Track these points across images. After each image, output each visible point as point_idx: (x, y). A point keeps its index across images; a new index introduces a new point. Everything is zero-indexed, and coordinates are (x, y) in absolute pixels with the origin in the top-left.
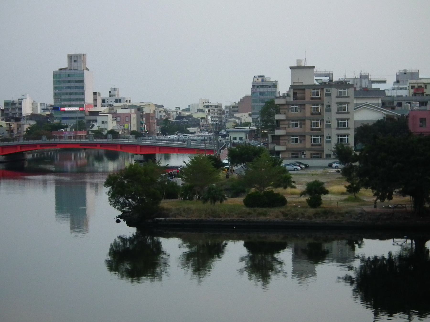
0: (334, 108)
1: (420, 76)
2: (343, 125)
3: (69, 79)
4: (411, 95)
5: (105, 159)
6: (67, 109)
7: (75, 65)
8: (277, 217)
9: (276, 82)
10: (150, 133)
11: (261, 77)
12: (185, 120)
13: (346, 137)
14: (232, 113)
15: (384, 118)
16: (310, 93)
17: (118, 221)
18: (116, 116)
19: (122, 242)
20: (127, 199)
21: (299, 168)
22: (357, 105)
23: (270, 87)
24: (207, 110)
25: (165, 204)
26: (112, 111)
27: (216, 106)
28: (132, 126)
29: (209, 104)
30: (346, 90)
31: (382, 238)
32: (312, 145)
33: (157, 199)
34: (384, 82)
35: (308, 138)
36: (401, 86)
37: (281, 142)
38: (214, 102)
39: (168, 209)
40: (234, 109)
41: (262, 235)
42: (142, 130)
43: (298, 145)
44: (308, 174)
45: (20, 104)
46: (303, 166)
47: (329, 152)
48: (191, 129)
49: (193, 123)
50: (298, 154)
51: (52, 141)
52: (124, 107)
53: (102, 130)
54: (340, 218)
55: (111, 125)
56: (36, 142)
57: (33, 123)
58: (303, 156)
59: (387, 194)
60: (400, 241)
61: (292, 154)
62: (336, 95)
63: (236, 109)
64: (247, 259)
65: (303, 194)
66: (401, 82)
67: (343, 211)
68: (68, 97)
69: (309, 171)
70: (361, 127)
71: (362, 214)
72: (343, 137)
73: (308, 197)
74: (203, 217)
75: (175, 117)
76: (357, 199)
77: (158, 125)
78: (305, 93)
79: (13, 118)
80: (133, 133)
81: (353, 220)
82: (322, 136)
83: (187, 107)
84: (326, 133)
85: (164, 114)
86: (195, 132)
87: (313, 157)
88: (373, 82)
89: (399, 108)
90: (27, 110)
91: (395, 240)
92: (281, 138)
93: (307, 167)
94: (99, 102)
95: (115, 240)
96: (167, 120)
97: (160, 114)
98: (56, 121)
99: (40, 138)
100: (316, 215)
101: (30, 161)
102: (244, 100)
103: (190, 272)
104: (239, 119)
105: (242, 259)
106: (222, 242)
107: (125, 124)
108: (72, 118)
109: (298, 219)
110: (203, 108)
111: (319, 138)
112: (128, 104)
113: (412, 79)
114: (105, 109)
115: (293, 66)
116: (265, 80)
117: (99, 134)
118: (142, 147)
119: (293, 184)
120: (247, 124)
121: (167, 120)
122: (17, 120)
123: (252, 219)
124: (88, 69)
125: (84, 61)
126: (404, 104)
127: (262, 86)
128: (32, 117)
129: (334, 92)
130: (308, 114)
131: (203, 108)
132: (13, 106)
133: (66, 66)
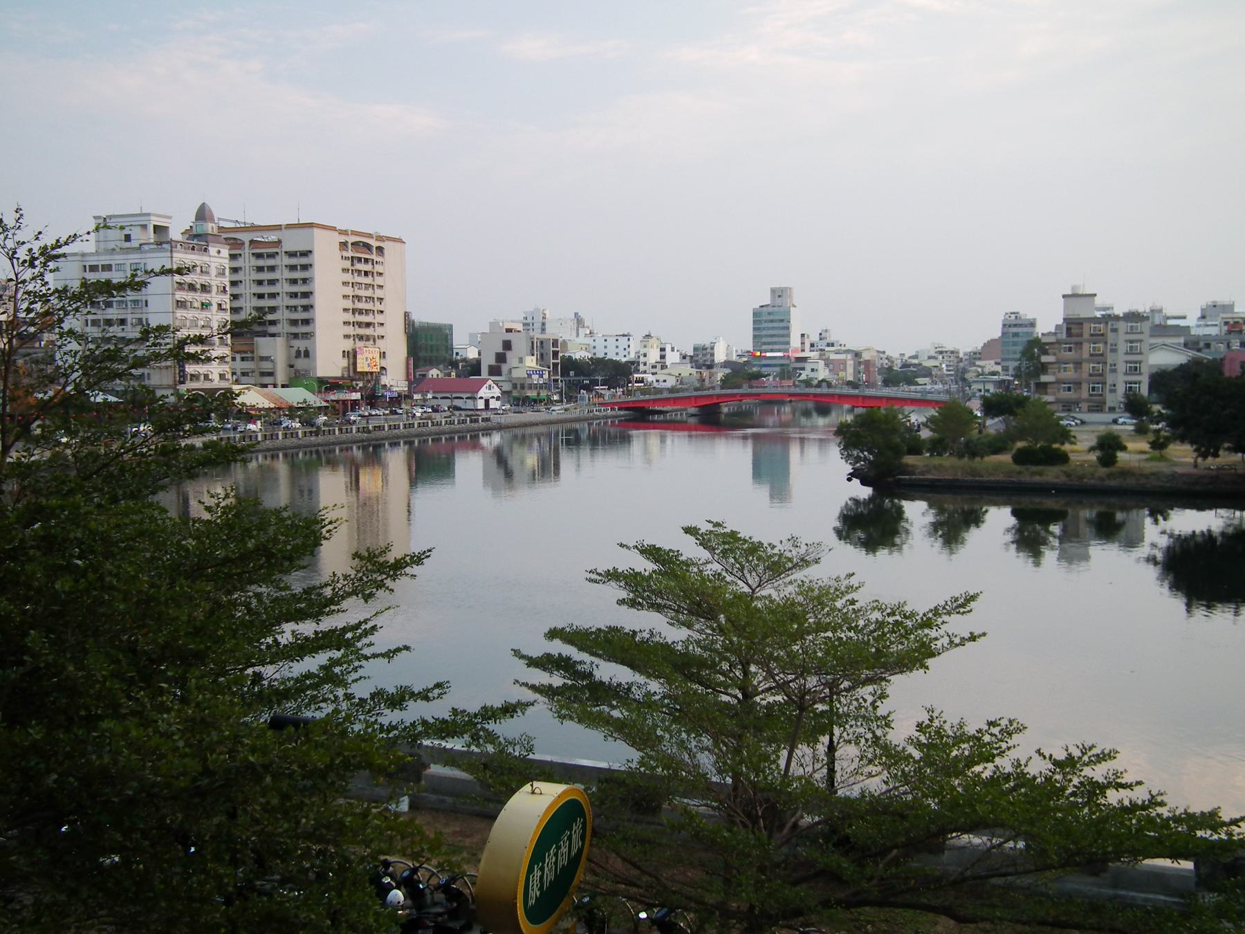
0: (1122, 347)
1: (1236, 310)
2: (1135, 370)
3: (771, 317)
4: (1223, 334)
5: (815, 415)
6: (768, 354)
7: (778, 301)
8: (1057, 477)
9: (1035, 319)
10: (870, 384)
11: (1014, 313)
12: (912, 369)
13: (1137, 385)
14: (974, 361)
15: (1189, 361)
16: (1087, 330)
17: (849, 480)
18: (828, 363)
19: (855, 504)
20: (862, 451)
21: (1073, 423)
22: (1151, 345)
23: (1026, 326)
24: (940, 357)
25: (909, 460)
26: (824, 357)
27: (952, 352)
28: (848, 375)
29: (944, 349)
30: (1139, 324)
31: (1200, 508)
32: (1091, 395)
33: (898, 452)
34: (1184, 318)
35: (1085, 386)
36: (1209, 323)
37: (1049, 390)
38: (949, 347)
39: (913, 466)
40: (975, 356)
41: (1037, 500)
42: (859, 380)
43: (1071, 395)
44: (1087, 431)
45: (712, 348)
46: (1079, 422)
47: (1112, 405)
48: (920, 380)
49: (922, 373)
50: (1070, 406)
51: (755, 391)
52: (837, 352)
53: (811, 379)
54: (1143, 481)
55: (823, 373)
56: (735, 391)
57: (728, 371)
58: (1077, 410)
59: (1212, 450)
60: (1222, 512)
61: (1064, 406)
62: (1125, 331)
63: (978, 356)
64: (1013, 531)
65: (1092, 449)
66: (1208, 318)
67: (1147, 471)
68: (769, 340)
69: (1086, 428)
70: (1157, 372)
71: (1174, 476)
72: (1133, 385)
73: (1098, 453)
74: (959, 476)
75: (900, 365)
76: (1162, 458)
77: (879, 374)
78: (1082, 328)
79: (704, 365)
80: (849, 383)
81: (1161, 484)
82: (1104, 383)
83: (914, 354)
84: (1110, 379)
85: (887, 361)
86: (925, 384)
87: (1090, 410)
88: (1168, 318)
89: (1207, 350)
90: (720, 357)
91: (1219, 511)
92: (1049, 386)
93: (1083, 423)
94: (807, 346)
95: (847, 504)
96: (890, 369)
97: (881, 361)
98: (755, 369)
99: (739, 387)
100: (1110, 476)
101: (727, 415)
102: (989, 345)
103: (939, 543)
104: (982, 367)
105: (1008, 530)
106: (981, 509)
107: (840, 373)
108: (775, 365)
109: (1085, 480)
110: (936, 355)
111: (1100, 385)
112: (843, 348)
113: (1224, 312)
114: (815, 355)
115: (1066, 293)
116: (1020, 318)
117: (808, 383)
118: (865, 397)
119: (1073, 439)
120: (994, 374)
121: (890, 369)
122: (710, 367)
123: (1023, 479)
124: (794, 306)
125: (790, 296)
126: (1213, 344)
127: (1015, 325)
128: (727, 364)
129: (1122, 326)
130: (1086, 355)
131: (936, 355)
132: (704, 352)
133: (768, 302)
